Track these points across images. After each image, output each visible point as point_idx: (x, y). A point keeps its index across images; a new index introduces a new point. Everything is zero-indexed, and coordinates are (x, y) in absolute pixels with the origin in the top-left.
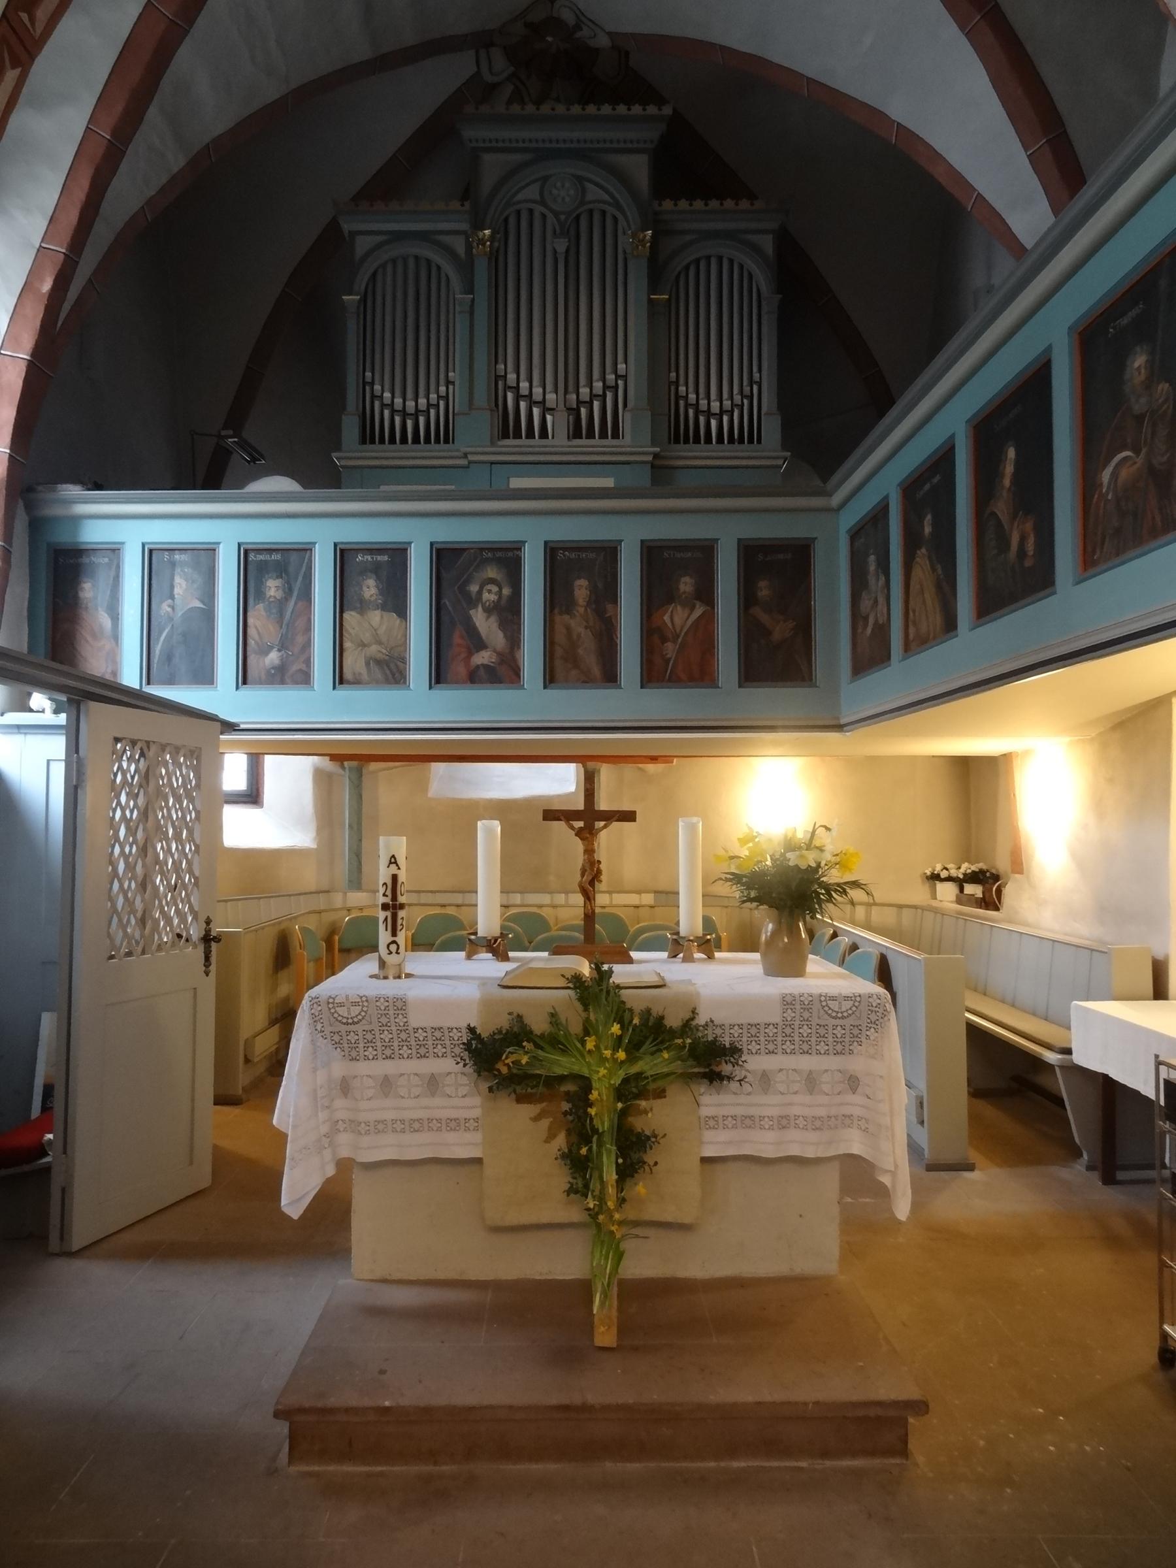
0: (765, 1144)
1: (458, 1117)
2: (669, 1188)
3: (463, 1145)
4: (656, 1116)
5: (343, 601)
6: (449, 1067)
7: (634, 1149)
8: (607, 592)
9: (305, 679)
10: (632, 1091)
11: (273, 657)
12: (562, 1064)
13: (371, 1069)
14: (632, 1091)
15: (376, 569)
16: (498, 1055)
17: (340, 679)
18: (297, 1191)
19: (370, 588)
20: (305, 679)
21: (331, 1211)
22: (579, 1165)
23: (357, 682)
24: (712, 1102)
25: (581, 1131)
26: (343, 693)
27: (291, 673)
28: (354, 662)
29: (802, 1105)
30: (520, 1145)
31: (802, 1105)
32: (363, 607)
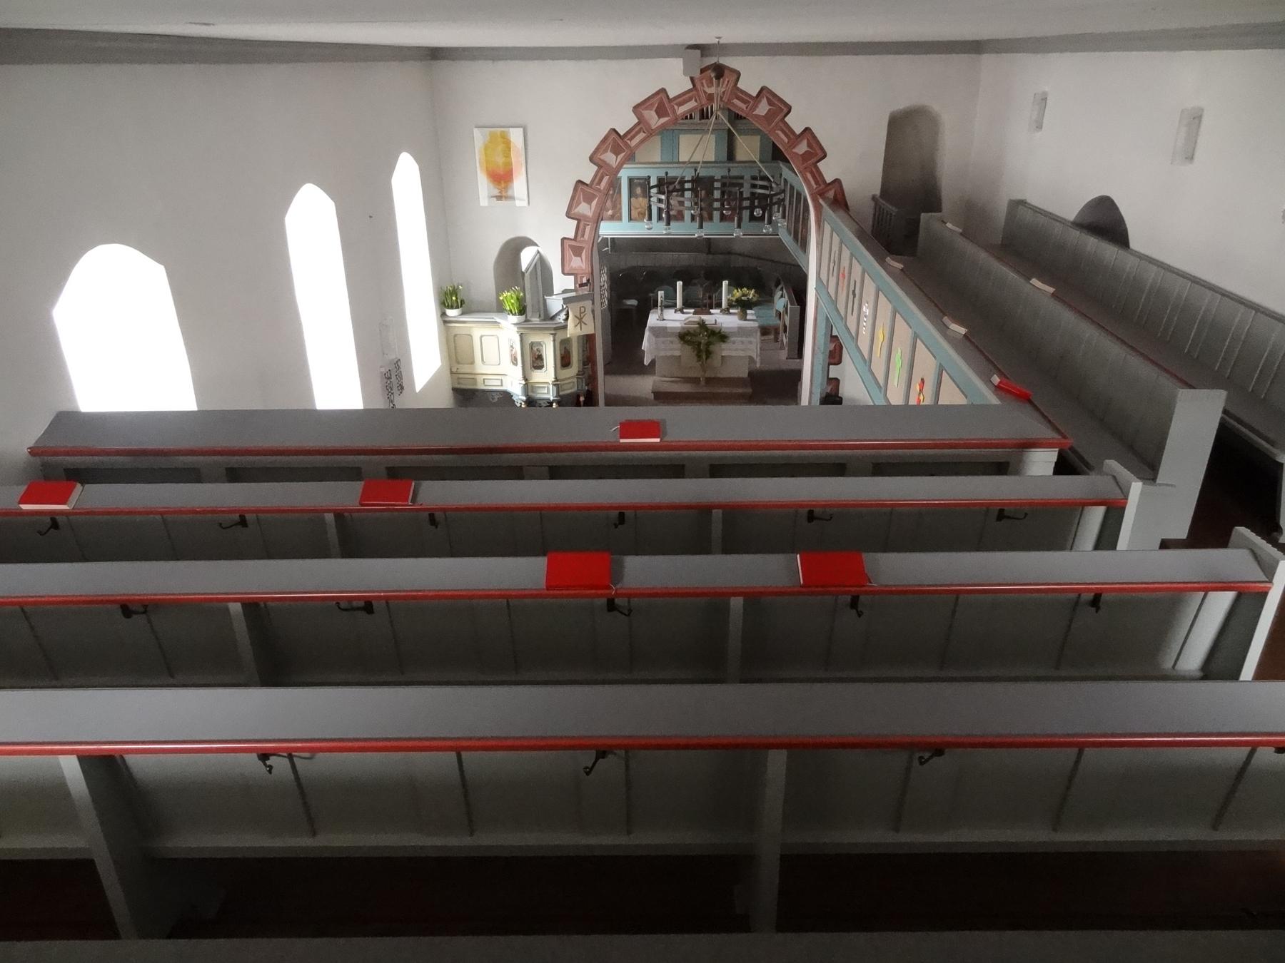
0: (734, 354)
1: (677, 349)
2: (716, 361)
3: (677, 353)
4: (712, 348)
5: (631, 194)
6: (676, 340)
7: (709, 353)
8: (710, 193)
9: (620, 219)
10: (708, 344)
11: (610, 212)
12: (695, 339)
13: (662, 339)
14: (708, 344)
15: (640, 185)
16: (685, 336)
17: (630, 219)
18: (646, 362)
19: (639, 191)
20: (620, 219)
21: (653, 363)
22: (699, 357)
23: (635, 220)
24: (724, 346)
25: (699, 351)
26: (632, 224)
27: (616, 217)
28: (635, 214)
29: (741, 346)
30: (686, 353)
31: (741, 346)
32: (637, 197)
